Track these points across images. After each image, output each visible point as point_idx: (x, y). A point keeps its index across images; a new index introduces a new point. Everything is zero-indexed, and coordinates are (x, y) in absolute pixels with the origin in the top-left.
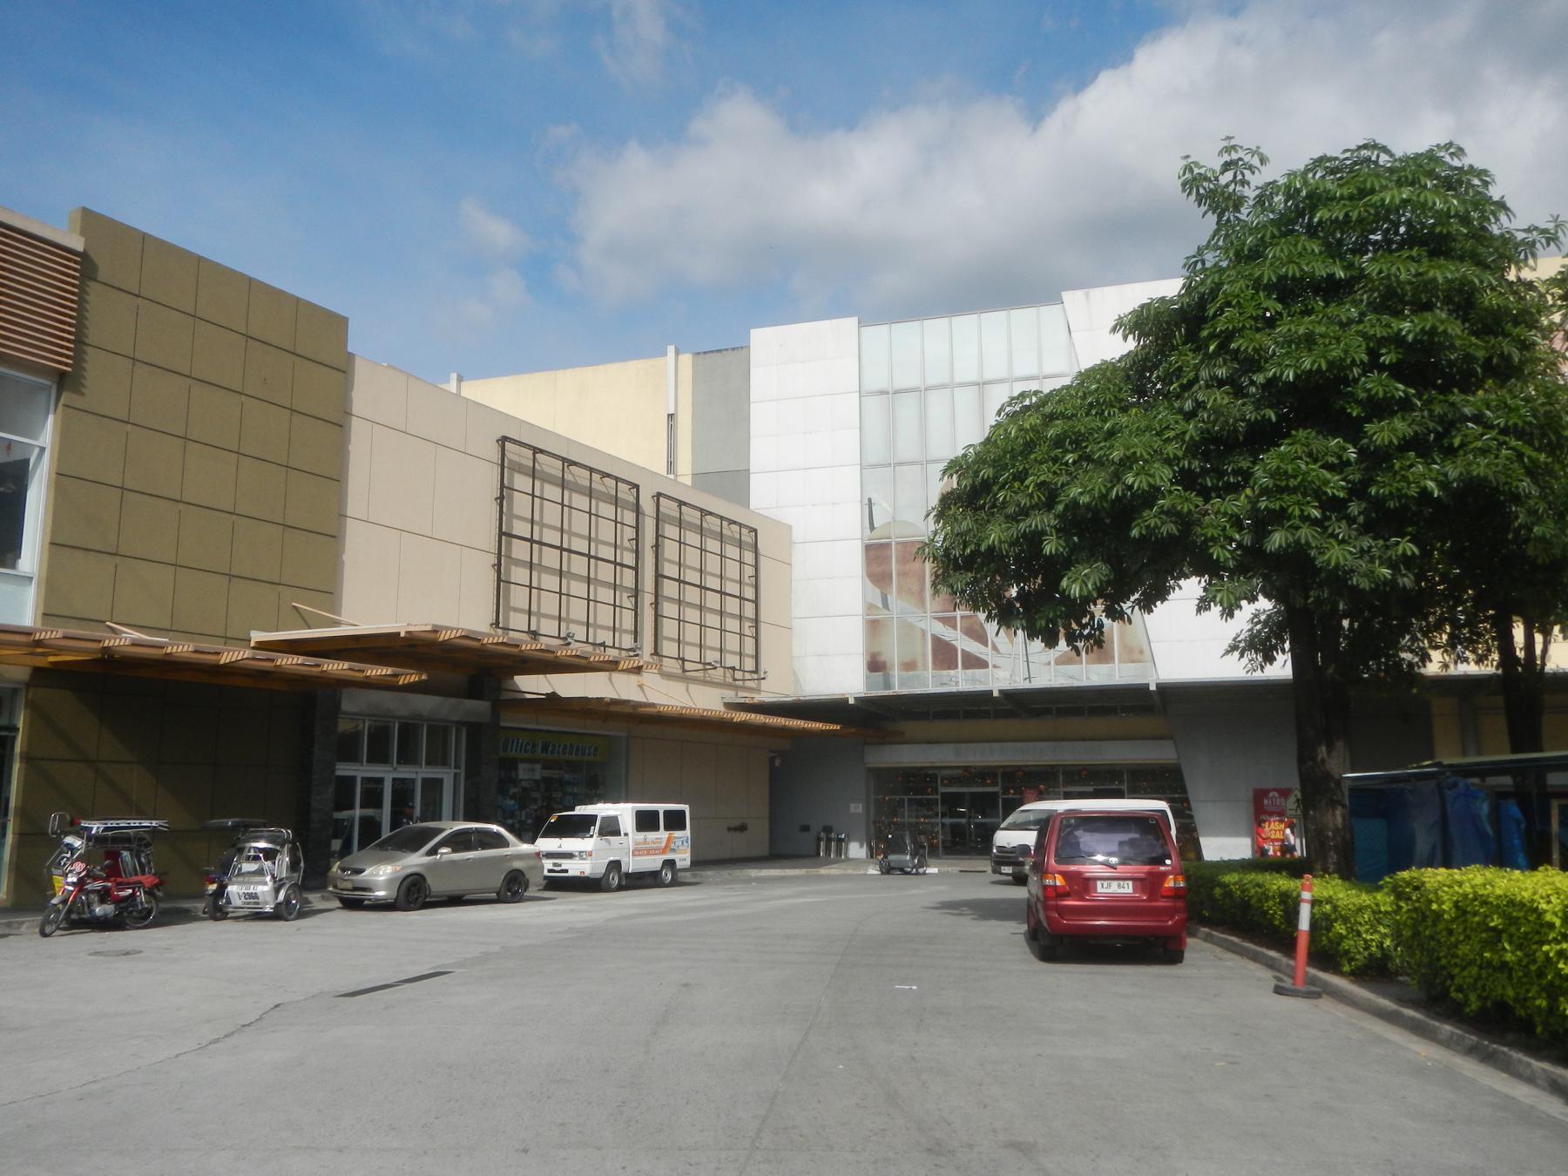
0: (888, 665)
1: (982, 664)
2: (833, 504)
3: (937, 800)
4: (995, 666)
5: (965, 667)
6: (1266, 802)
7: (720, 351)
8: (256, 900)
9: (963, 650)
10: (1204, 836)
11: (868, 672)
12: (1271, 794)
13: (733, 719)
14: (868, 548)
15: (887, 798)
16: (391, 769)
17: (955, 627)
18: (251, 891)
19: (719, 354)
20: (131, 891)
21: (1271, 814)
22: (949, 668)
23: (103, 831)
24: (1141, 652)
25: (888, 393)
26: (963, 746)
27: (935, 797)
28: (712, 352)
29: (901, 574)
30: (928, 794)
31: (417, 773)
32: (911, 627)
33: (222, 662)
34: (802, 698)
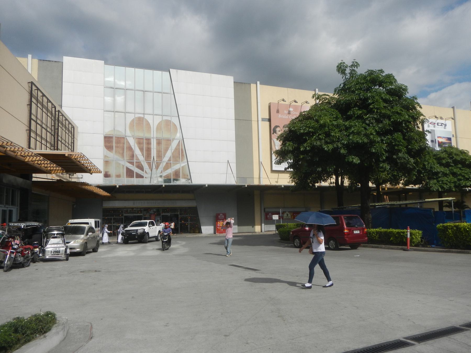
0: (111, 175)
1: (142, 177)
2: (94, 121)
3: (123, 218)
4: (146, 178)
5: (137, 177)
6: (219, 217)
7: (50, 61)
8: (58, 253)
9: (136, 172)
10: (203, 226)
11: (104, 177)
12: (220, 215)
13: (94, 191)
14: (105, 137)
15: (106, 218)
16: (3, 206)
17: (133, 165)
18: (58, 250)
19: (49, 62)
20: (27, 251)
21: (220, 220)
22: (131, 177)
23: (26, 227)
24: (187, 176)
25: (113, 88)
26: (136, 201)
27: (122, 217)
28: (47, 61)
29: (117, 147)
30: (120, 216)
31: (7, 207)
32: (120, 164)
33: (26, 160)
34: (100, 185)
